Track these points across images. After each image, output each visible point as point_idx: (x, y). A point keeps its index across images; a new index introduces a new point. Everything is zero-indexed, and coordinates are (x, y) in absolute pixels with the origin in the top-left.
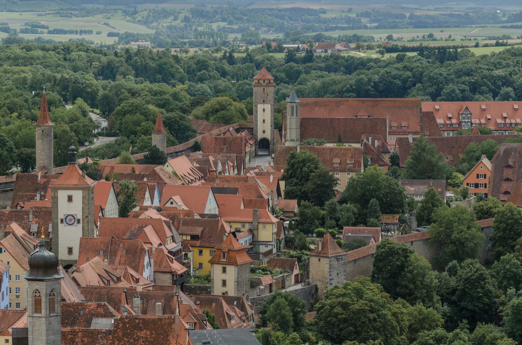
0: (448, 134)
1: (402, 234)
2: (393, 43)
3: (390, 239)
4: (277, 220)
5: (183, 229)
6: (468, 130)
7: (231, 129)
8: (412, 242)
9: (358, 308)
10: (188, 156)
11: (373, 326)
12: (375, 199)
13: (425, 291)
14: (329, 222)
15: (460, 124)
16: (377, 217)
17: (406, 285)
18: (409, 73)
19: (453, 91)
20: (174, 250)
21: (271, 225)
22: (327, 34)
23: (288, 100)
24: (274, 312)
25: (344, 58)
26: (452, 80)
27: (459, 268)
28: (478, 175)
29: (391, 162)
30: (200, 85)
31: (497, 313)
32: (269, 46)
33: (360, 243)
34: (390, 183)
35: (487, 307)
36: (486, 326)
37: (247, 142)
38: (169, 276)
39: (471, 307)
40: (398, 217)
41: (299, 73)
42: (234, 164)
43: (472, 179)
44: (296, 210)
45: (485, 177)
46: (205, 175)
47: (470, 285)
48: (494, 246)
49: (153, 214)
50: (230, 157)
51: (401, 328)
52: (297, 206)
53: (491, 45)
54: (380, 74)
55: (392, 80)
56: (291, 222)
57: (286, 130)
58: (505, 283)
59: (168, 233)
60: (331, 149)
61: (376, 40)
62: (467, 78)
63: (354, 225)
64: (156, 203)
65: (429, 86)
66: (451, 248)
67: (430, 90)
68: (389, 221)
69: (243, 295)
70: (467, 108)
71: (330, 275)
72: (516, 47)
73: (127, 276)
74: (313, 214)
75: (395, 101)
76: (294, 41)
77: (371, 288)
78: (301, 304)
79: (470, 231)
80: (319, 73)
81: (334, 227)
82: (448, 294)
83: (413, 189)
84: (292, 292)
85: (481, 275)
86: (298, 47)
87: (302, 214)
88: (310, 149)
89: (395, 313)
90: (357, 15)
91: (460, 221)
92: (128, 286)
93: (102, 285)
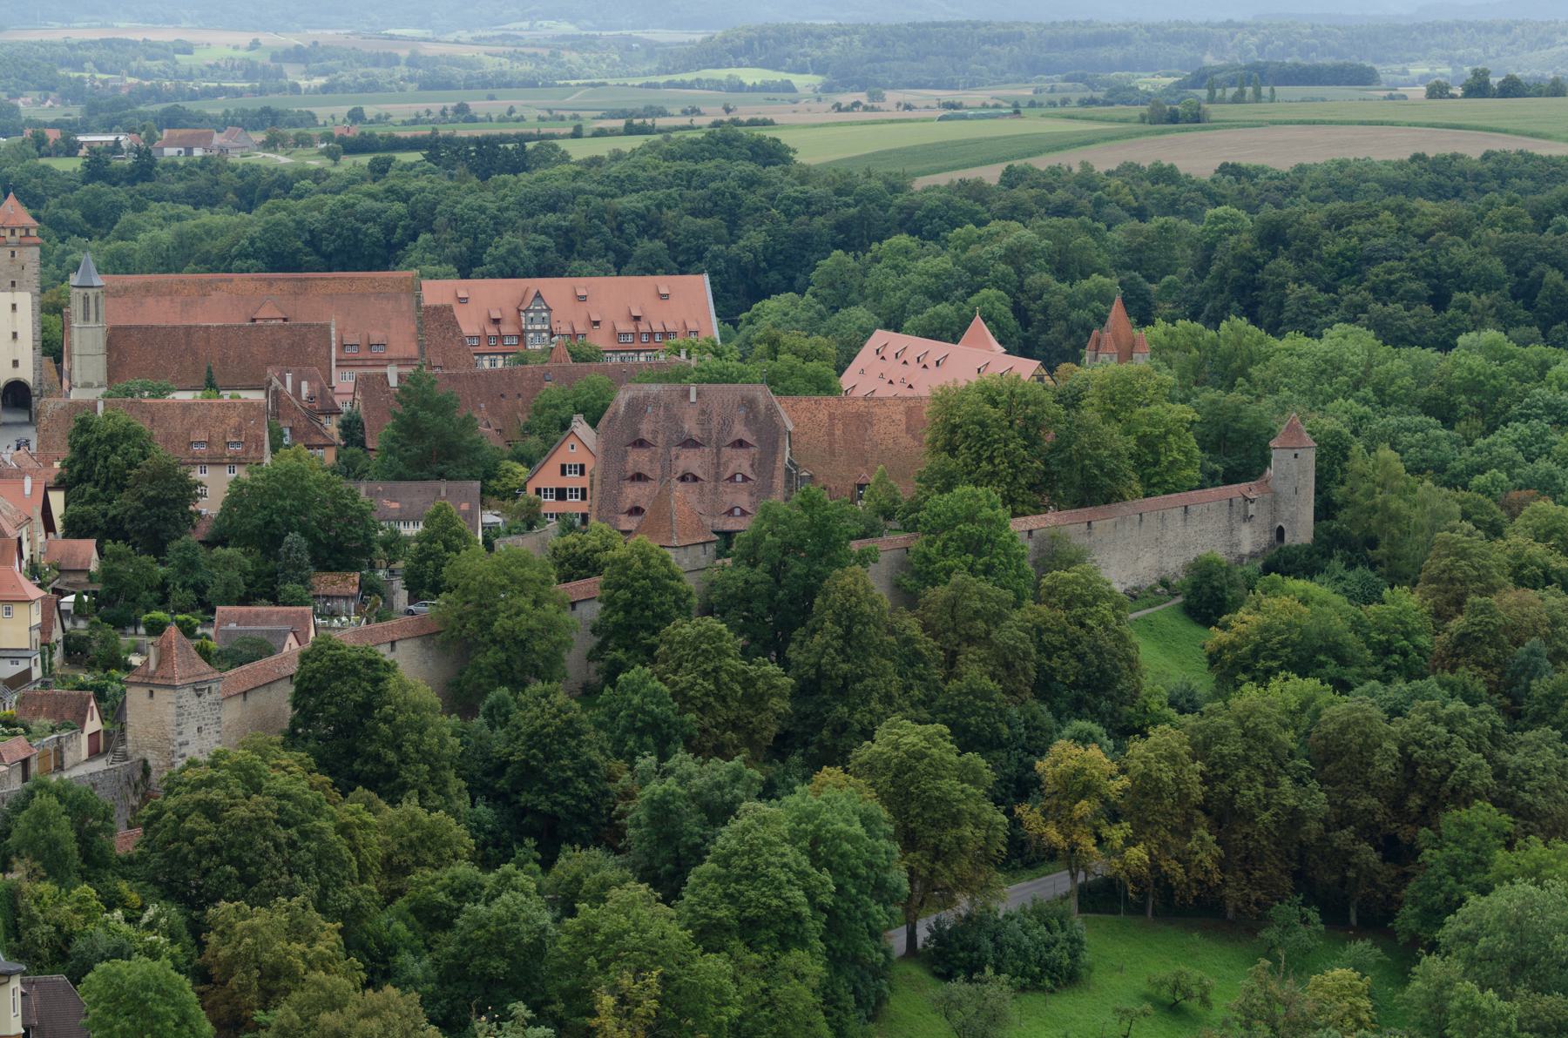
1: (368, 622)
2: (367, 129)
3: (336, 635)
4: (42, 593)
6: (543, 352)
8: (393, 643)
9: (248, 814)
11: (286, 862)
12: (297, 534)
13: (427, 767)
14: (178, 595)
15: (521, 337)
16: (303, 581)
17: (379, 755)
18: (399, 207)
19: (513, 252)
21: (26, 606)
22: (192, 106)
23: (74, 279)
24: (30, 832)
25: (233, 169)
26: (512, 225)
27: (513, 706)
28: (563, 467)
29: (344, 437)
31: (611, 820)
32: (40, 142)
33: (261, 649)
34: (334, 492)
35: (586, 806)
36: (584, 853)
39: (545, 806)
40: (357, 579)
41: (117, 208)
43: (549, 477)
44: (94, 567)
45: (582, 473)
47: (543, 750)
48: (602, 647)
51: (361, 866)
52: (95, 555)
53: (613, 133)
54: (326, 209)
55: (358, 225)
56: (79, 597)
57: (70, 359)
58: (631, 743)
60: (186, 407)
61: (321, 122)
62: (551, 218)
63: (244, 601)
65: (452, 240)
66: (493, 656)
67: (454, 249)
68: (334, 590)
70: (538, 296)
71: (180, 733)
72: (674, 135)
74: (136, 574)
75: (352, 279)
76: (108, 127)
77: (284, 763)
78: (101, 809)
79: (539, 612)
80: (170, 208)
81: (193, 609)
82: (487, 774)
83: (396, 505)
85: (570, 722)
86: (117, 142)
87: (107, 576)
88: (129, 408)
90: (274, 57)
91: (519, 584)
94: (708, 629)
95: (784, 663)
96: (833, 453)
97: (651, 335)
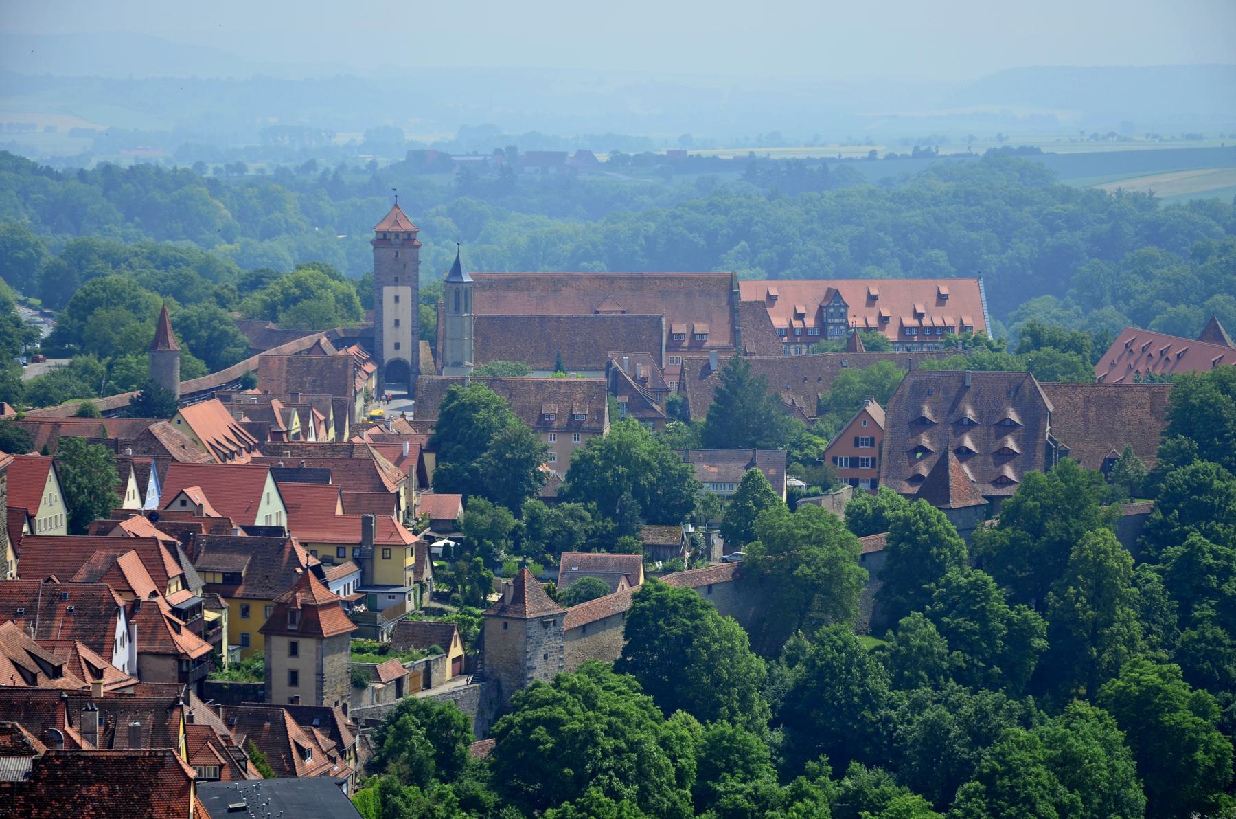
0: (798, 351)
5: (205, 558)
7: (324, 340)
10: (225, 399)
20: (184, 607)
28: (856, 440)
30: (267, 244)
37: (359, 368)
38: (171, 663)
42: (327, 416)
45: (872, 445)
46: (262, 438)
49: (140, 527)
50: (319, 401)
52: (461, 508)
59: (172, 569)
60: (540, 385)
63: (585, 549)
64: (153, 502)
69: (337, 703)
73: (78, 665)
83: (714, 470)
84: (443, 696)
89: (667, 738)
92: (77, 684)
93: (21, 683)
94: (977, 580)
95: (1041, 608)
96: (1087, 431)
97: (933, 329)
